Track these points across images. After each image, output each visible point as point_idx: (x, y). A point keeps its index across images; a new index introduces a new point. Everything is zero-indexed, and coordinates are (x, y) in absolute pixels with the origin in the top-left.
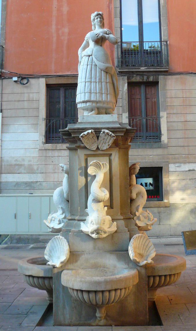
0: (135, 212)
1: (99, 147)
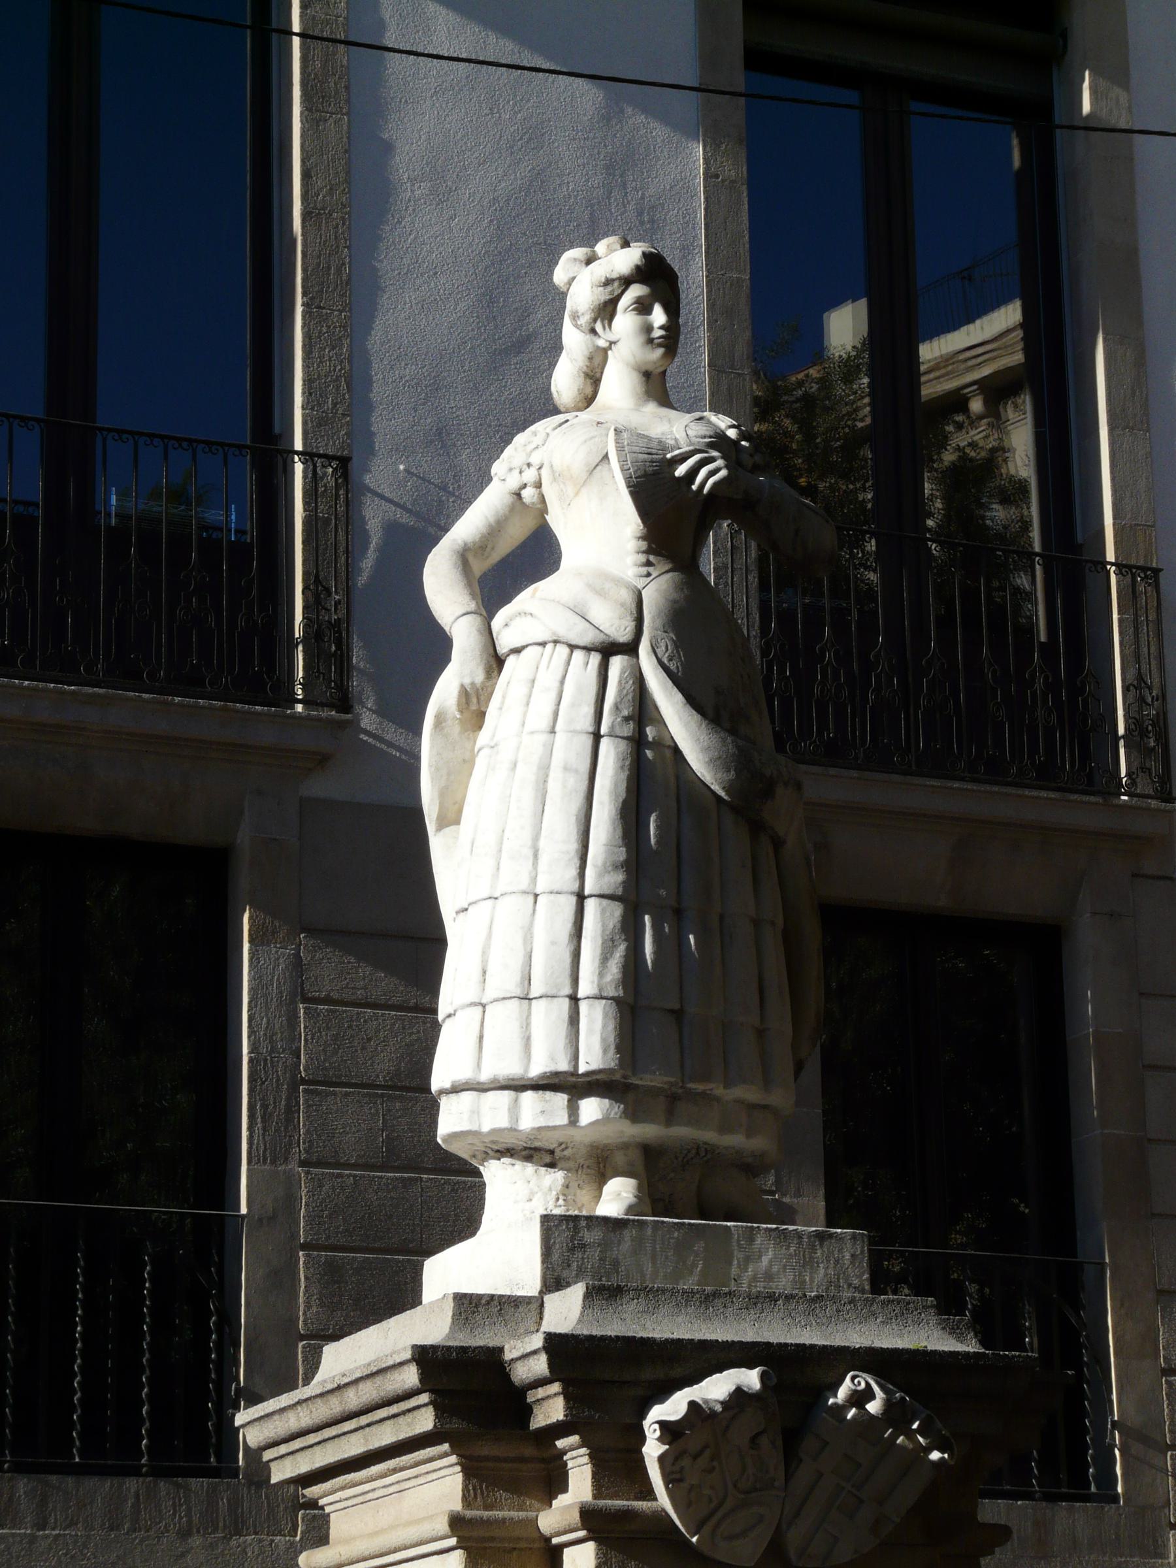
1: (794, 1537)
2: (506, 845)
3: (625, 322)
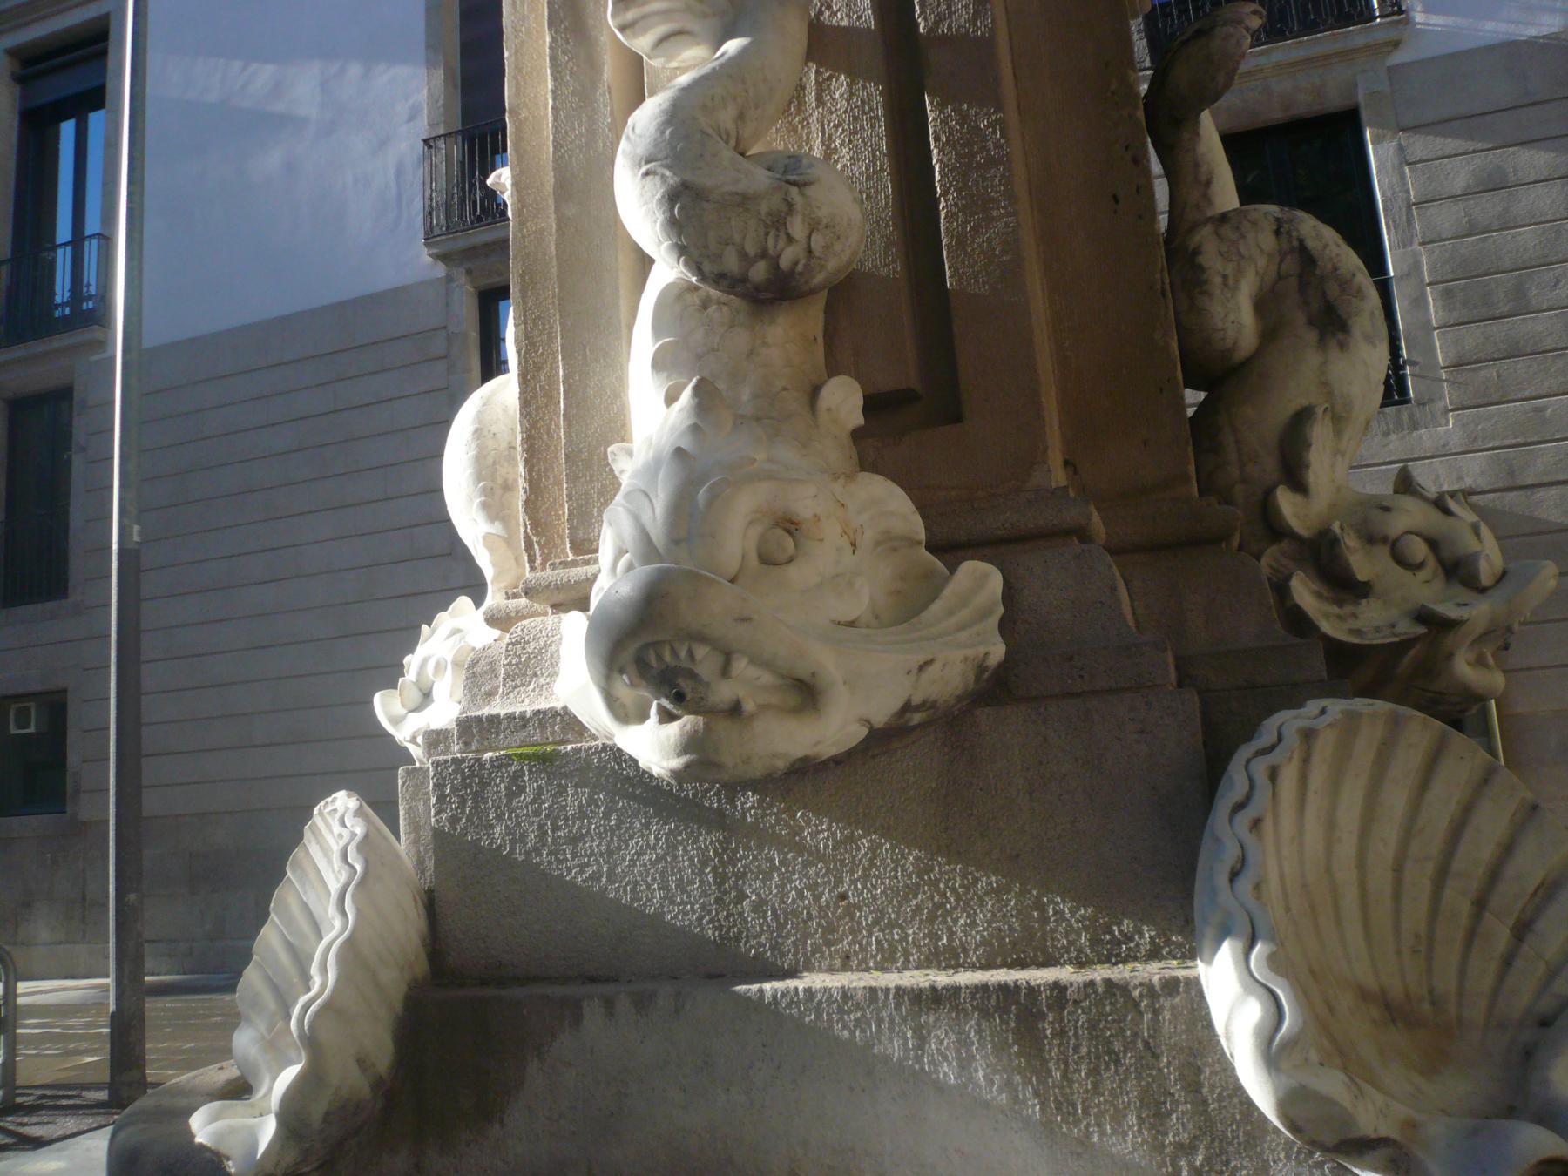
0: (1269, 493)
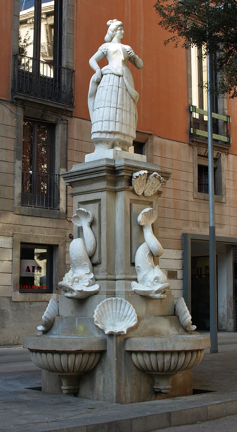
1: (145, 192)
2: (106, 100)
3: (118, 32)
